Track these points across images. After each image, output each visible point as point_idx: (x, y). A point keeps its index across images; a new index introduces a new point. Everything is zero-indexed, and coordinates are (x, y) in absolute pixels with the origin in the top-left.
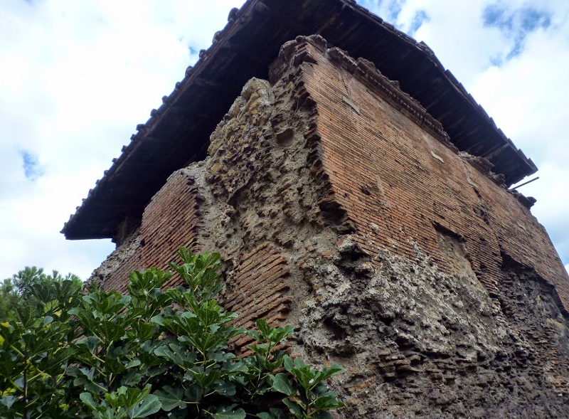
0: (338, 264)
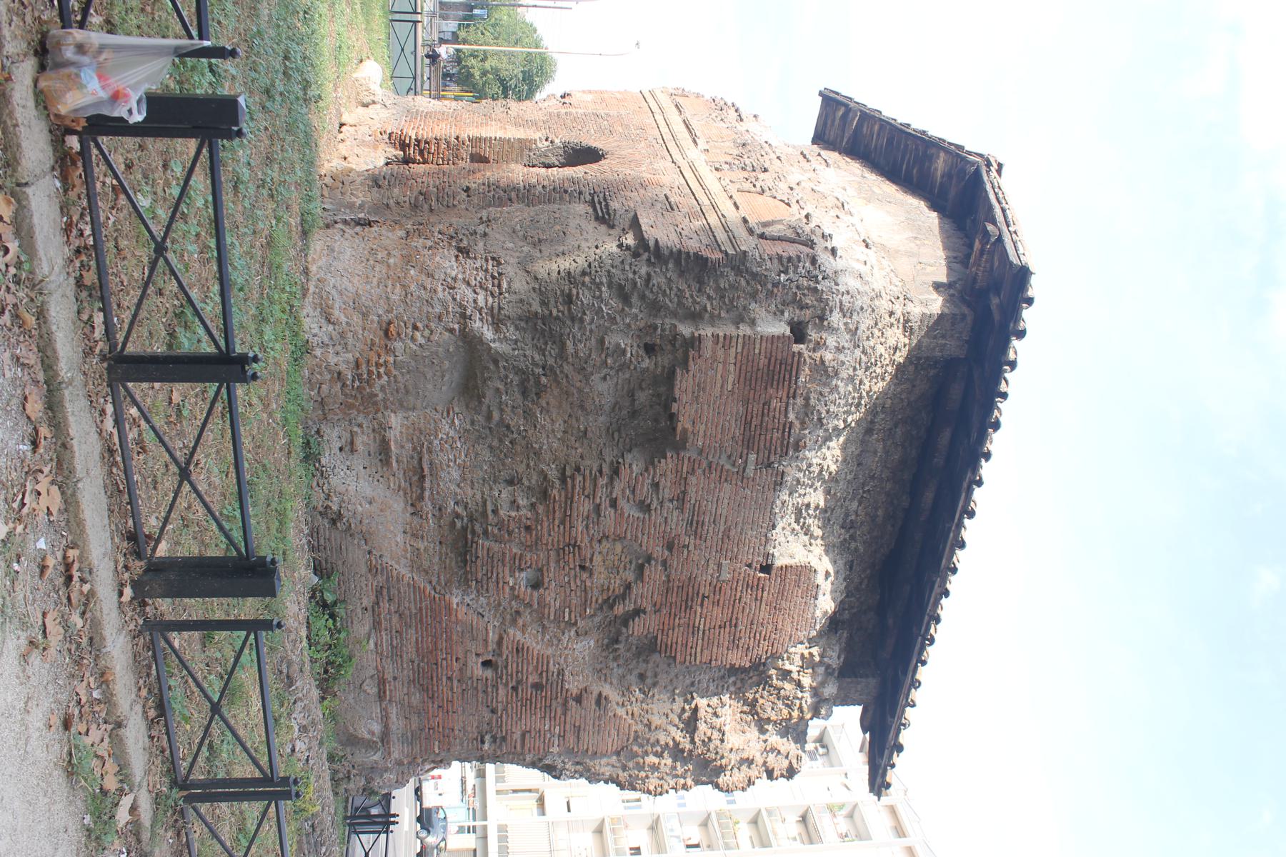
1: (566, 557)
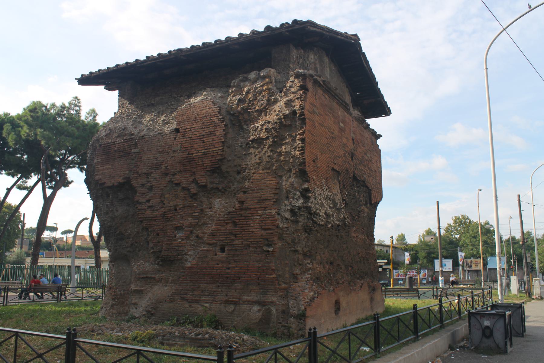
0: (301, 192)
1: (168, 217)
